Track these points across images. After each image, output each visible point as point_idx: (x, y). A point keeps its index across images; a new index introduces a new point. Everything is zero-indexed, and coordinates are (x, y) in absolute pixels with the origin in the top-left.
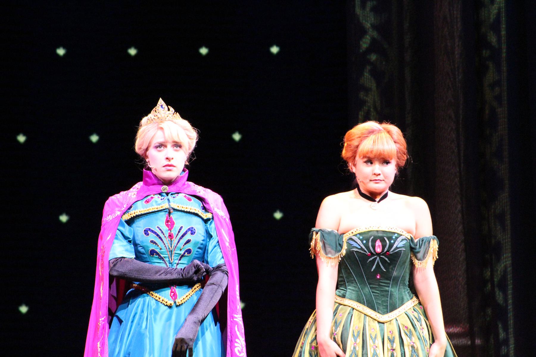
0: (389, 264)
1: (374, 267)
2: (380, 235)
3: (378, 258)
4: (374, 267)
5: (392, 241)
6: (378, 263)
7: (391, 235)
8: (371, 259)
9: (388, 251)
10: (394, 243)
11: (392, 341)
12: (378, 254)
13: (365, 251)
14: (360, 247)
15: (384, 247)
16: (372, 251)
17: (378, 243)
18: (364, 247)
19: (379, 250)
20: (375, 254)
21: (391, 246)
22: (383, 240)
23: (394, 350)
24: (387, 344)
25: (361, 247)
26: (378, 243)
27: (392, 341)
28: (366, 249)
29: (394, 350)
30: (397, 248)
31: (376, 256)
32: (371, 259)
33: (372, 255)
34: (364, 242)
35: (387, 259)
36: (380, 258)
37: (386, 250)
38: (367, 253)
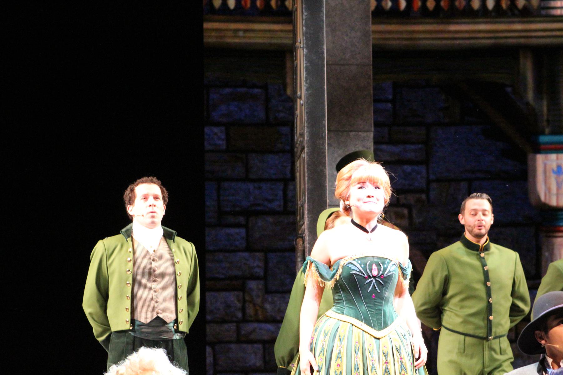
0: (383, 286)
1: (370, 288)
2: (375, 260)
3: (374, 280)
4: (370, 288)
5: (385, 266)
6: (374, 285)
7: (384, 261)
8: (368, 281)
9: (382, 274)
10: (387, 267)
11: (386, 356)
12: (374, 277)
13: (364, 274)
14: (359, 270)
15: (379, 270)
16: (370, 274)
17: (374, 267)
18: (362, 270)
19: (375, 273)
20: (372, 276)
21: (385, 270)
22: (378, 265)
23: (388, 363)
24: (382, 358)
25: (360, 270)
26: (374, 267)
27: (386, 356)
28: (364, 272)
29: (388, 363)
30: (389, 272)
31: (372, 279)
32: (368, 281)
33: (369, 277)
34: (363, 266)
35: (381, 281)
36: (376, 280)
37: (381, 273)
38: (365, 275)
